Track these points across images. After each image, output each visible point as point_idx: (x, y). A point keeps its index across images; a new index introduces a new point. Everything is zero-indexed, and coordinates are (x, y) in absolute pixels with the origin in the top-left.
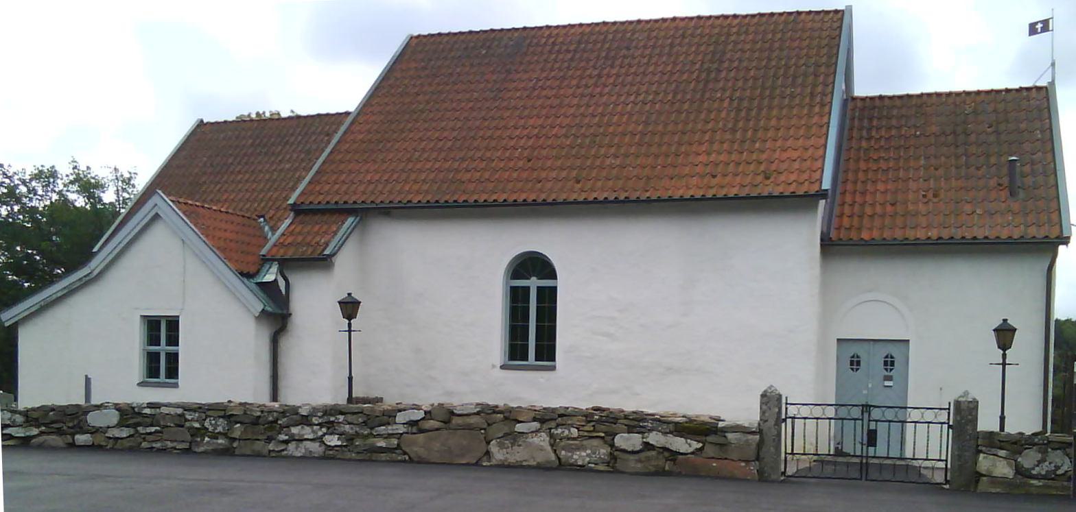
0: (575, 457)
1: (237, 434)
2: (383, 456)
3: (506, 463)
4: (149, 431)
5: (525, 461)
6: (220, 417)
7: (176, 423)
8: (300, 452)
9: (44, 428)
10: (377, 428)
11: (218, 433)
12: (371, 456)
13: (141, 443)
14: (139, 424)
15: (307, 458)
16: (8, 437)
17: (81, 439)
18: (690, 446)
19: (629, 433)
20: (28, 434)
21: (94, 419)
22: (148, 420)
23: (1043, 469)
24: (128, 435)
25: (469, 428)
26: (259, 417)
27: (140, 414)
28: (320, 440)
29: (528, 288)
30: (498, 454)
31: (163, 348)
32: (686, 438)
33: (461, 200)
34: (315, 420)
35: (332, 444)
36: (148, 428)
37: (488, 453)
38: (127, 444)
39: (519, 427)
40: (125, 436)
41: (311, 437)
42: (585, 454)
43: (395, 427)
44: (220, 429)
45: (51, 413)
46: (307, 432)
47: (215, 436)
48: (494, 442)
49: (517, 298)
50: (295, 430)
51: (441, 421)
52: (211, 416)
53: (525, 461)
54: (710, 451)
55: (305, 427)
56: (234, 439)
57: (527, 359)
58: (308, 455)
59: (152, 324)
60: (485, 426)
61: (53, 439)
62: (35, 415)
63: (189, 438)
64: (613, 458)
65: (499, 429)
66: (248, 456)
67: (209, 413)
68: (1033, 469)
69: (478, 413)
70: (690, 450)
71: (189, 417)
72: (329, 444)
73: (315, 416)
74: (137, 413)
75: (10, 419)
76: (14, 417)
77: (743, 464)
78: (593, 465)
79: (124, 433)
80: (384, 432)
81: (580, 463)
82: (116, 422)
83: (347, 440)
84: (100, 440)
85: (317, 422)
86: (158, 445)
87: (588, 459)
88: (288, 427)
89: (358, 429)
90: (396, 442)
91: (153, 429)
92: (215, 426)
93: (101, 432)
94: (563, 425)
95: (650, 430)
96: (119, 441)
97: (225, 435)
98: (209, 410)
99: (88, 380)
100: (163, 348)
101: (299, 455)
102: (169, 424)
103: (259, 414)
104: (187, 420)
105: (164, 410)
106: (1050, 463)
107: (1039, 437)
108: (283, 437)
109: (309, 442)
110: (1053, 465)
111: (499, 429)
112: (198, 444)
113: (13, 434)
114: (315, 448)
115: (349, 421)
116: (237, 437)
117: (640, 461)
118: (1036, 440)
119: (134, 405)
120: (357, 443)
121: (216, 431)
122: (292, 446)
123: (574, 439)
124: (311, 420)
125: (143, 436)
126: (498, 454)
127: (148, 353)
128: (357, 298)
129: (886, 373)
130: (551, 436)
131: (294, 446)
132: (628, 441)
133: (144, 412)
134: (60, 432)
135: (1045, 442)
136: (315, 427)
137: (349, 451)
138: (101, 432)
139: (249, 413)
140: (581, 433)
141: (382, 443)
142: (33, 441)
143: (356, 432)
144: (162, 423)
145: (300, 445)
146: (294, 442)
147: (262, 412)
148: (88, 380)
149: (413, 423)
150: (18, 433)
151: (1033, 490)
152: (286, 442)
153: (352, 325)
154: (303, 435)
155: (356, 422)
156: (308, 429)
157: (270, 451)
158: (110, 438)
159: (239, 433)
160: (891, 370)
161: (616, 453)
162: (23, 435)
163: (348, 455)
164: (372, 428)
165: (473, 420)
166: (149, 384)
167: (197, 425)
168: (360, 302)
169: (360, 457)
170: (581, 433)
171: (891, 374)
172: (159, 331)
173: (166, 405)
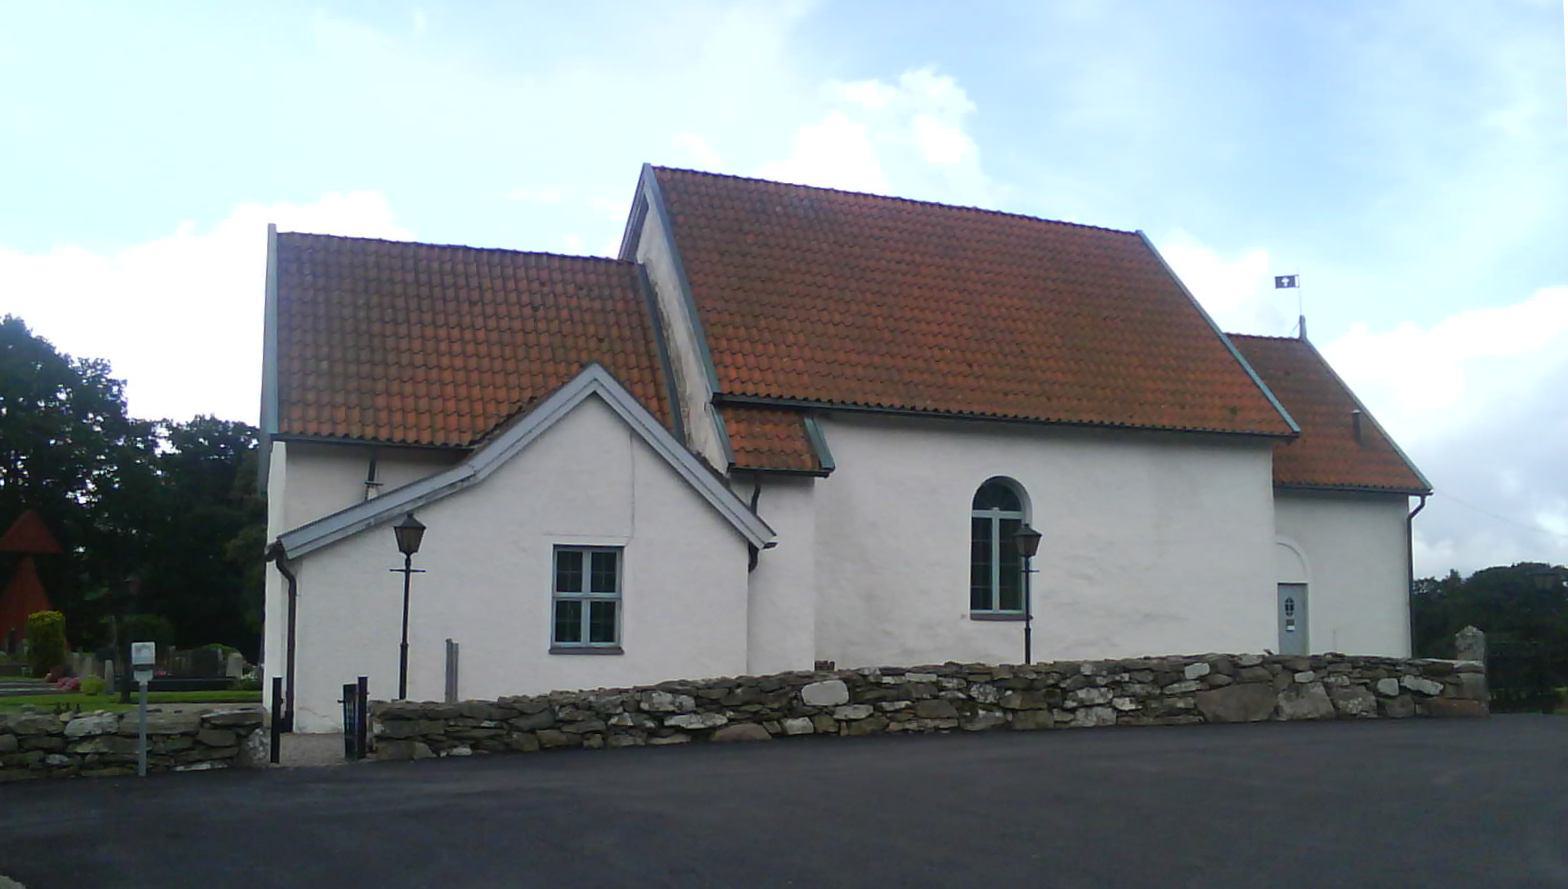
0: (1350, 706)
1: (1016, 703)
2: (1183, 719)
3: (1295, 717)
4: (898, 707)
5: (1309, 713)
6: (987, 683)
7: (932, 693)
8: (1091, 721)
9: (732, 713)
10: (1170, 687)
11: (989, 704)
12: (1170, 719)
13: (888, 725)
14: (883, 699)
15: (1100, 728)
16: (672, 731)
17: (797, 725)
18: (1437, 687)
19: (1389, 677)
20: (709, 723)
21: (812, 694)
22: (893, 692)
24: (867, 714)
25: (1258, 680)
26: (1033, 680)
27: (879, 684)
28: (1109, 704)
29: (989, 520)
30: (1288, 709)
31: (586, 595)
32: (1432, 680)
33: (930, 408)
34: (1100, 680)
35: (1126, 708)
36: (896, 703)
37: (1277, 710)
38: (869, 728)
39: (1299, 677)
40: (863, 716)
41: (1101, 701)
42: (1356, 702)
43: (1188, 684)
44: (991, 699)
45: (739, 690)
46: (1095, 695)
47: (989, 708)
48: (1280, 695)
49: (980, 528)
50: (1082, 694)
51: (1228, 675)
52: (975, 683)
53: (1309, 713)
54: (1451, 690)
55: (1092, 690)
56: (1014, 711)
57: (989, 607)
58: (1101, 724)
59: (567, 560)
60: (1271, 678)
61: (750, 729)
62: (715, 694)
63: (955, 712)
64: (1380, 706)
65: (1283, 680)
66: (1032, 730)
67: (971, 678)
69: (1261, 665)
70: (1437, 692)
71: (950, 685)
72: (1123, 708)
73: (1100, 676)
74: (872, 683)
75: (672, 703)
76: (678, 700)
77: (1476, 702)
78: (1365, 714)
79: (862, 712)
80: (1178, 691)
81: (1354, 712)
82: (848, 698)
83: (1139, 703)
84: (826, 724)
85: (1103, 683)
86: (913, 726)
87: (1360, 707)
88: (1072, 691)
89: (1149, 689)
90: (1192, 702)
91: (903, 704)
92: (986, 695)
93: (826, 713)
94: (1336, 672)
95: (1405, 675)
96: (854, 724)
97: (996, 705)
98: (970, 674)
99: (452, 649)
100: (586, 595)
101: (1092, 724)
102: (925, 696)
103: (1034, 676)
104: (943, 689)
105: (909, 677)
108: (1070, 704)
109: (1099, 709)
111: (1283, 680)
112: (970, 720)
113: (684, 725)
114: (1108, 714)
115: (1140, 679)
116: (1017, 708)
117: (1403, 706)
119: (866, 673)
120: (1153, 706)
121: (988, 702)
122: (1081, 714)
123: (1346, 687)
124: (1095, 681)
125: (889, 715)
126: (1288, 709)
127: (557, 602)
128: (1037, 530)
129: (1288, 618)
130: (1327, 686)
131: (1084, 714)
132: (1387, 685)
133: (884, 681)
134: (758, 719)
136: (1103, 690)
137: (1144, 715)
138: (826, 713)
139: (1021, 675)
140: (1353, 681)
141: (1181, 704)
142: (719, 734)
143: (1148, 692)
144: (915, 695)
145: (1090, 712)
146: (1082, 710)
147: (1037, 673)
148: (452, 649)
149: (1201, 679)
150: (691, 723)
152: (1073, 710)
153: (412, 562)
154: (1093, 700)
155: (1146, 681)
156: (1094, 693)
157: (1056, 722)
158: (842, 720)
159: (1018, 702)
160: (1292, 614)
161: (1381, 700)
162: (702, 726)
163: (1145, 720)
164: (1162, 688)
165: (1260, 672)
166: (599, 651)
167: (961, 695)
168: (1040, 536)
169: (1159, 721)
170: (1353, 681)
171: (1293, 617)
172: (580, 568)
173: (909, 671)
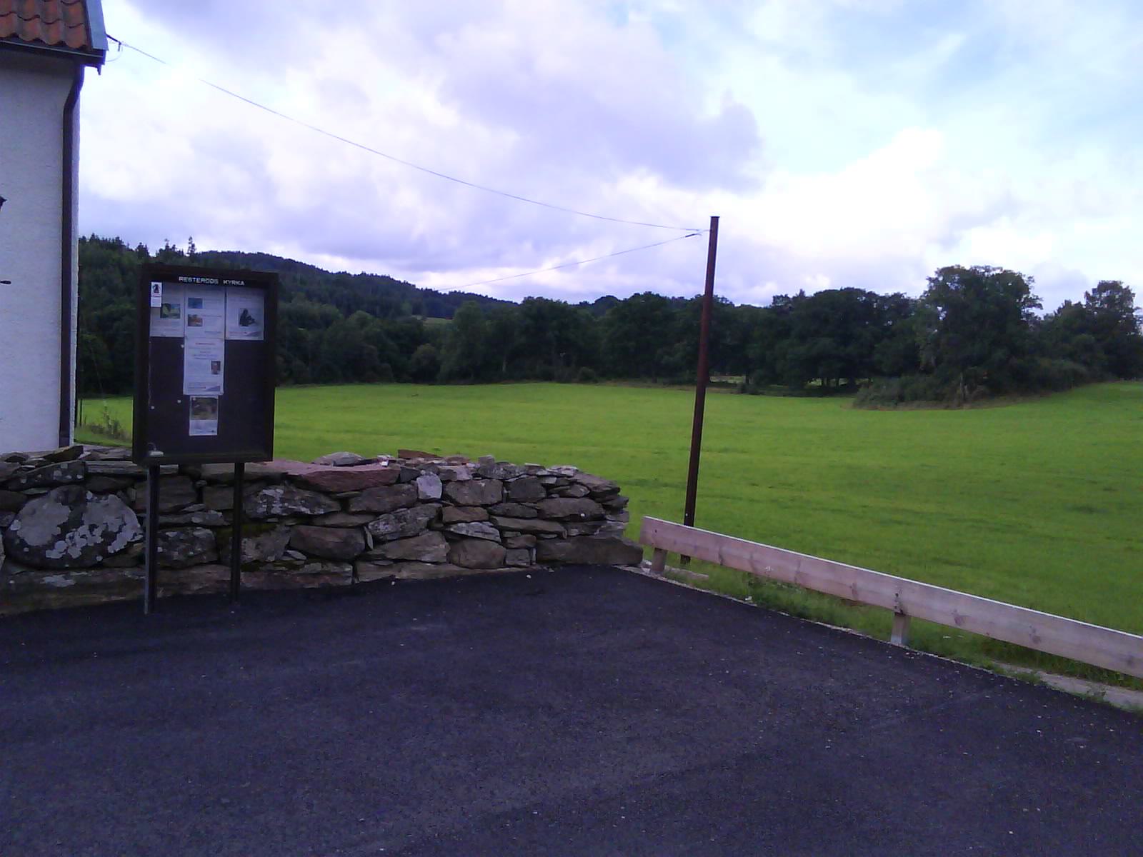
23: (79, 541)
68: (51, 546)
106: (92, 527)
107: (64, 465)
110: (98, 532)
118: (57, 473)
135: (80, 477)
151: (53, 601)
